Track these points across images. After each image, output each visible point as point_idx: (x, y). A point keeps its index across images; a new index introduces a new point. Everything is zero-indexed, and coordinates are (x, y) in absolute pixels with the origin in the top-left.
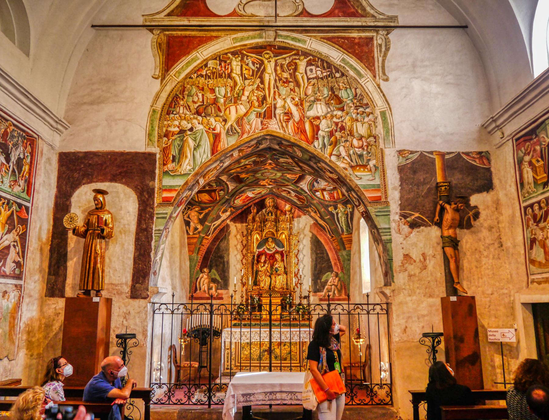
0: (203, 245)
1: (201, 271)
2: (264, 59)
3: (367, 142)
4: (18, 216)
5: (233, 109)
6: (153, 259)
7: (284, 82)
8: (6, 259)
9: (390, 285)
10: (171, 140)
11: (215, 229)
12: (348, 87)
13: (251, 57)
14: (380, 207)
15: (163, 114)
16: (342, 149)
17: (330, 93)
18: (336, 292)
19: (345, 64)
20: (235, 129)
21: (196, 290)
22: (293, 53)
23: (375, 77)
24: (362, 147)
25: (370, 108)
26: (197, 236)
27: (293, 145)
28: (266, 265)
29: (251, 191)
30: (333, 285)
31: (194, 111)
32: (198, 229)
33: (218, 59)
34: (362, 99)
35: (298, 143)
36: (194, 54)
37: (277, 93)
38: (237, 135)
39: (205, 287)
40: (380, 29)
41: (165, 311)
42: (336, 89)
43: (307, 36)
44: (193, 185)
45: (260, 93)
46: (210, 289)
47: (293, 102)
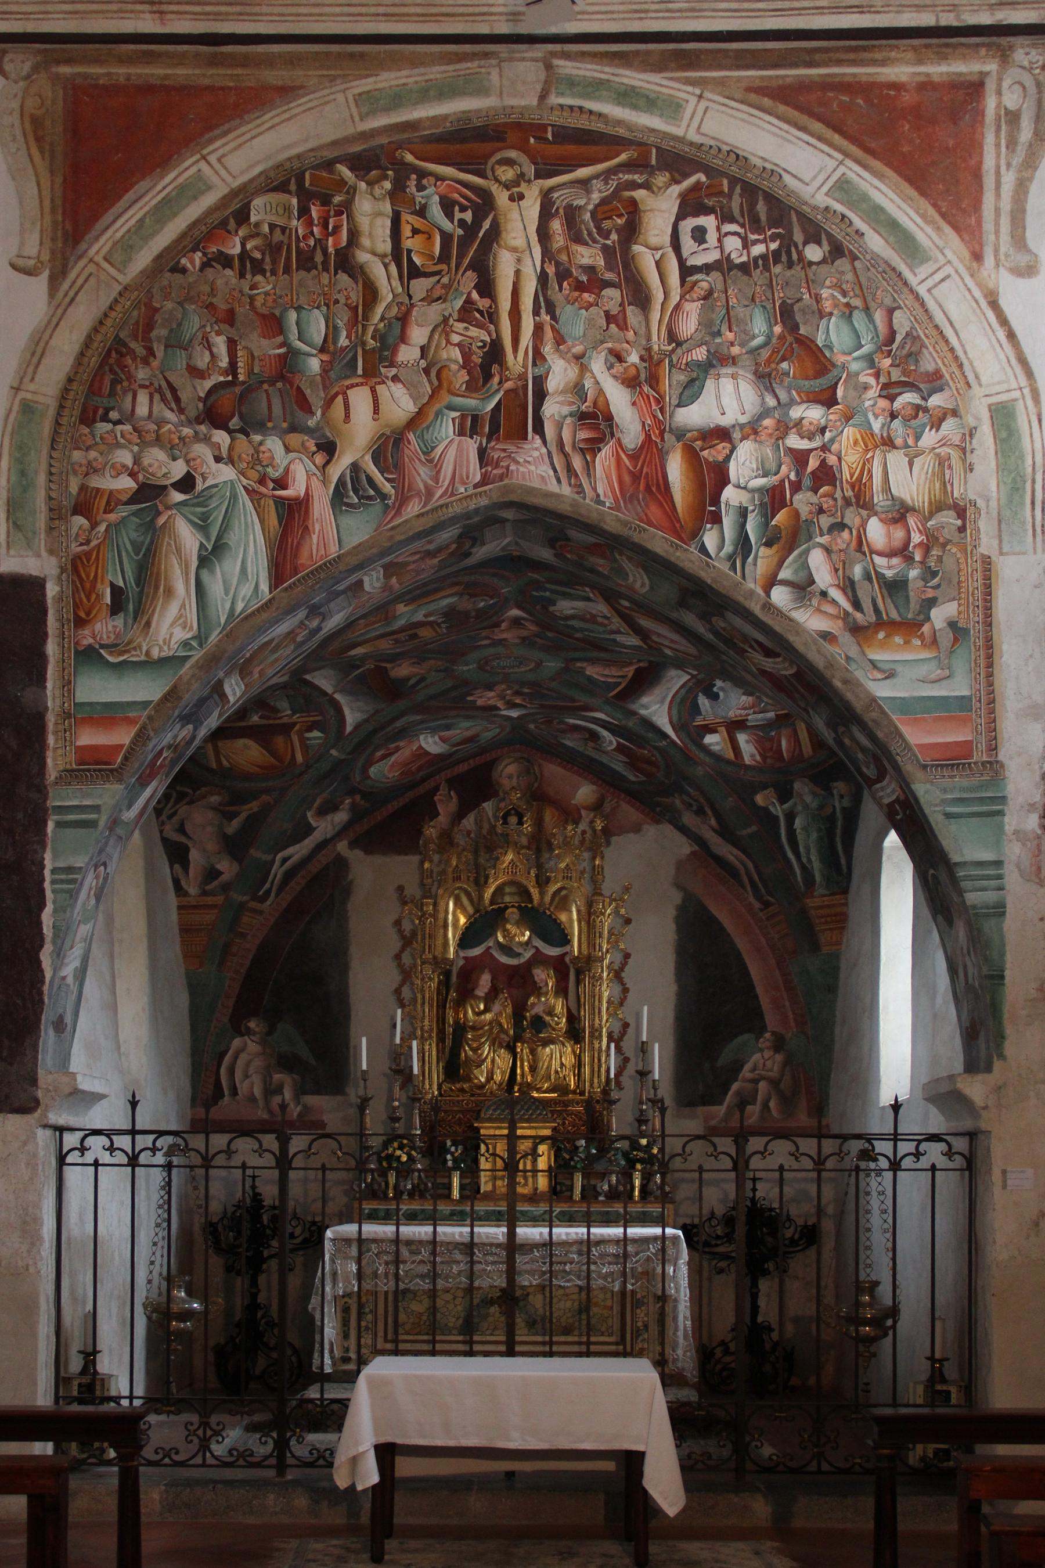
0: (243, 936)
1: (238, 1028)
2: (495, 188)
3: (925, 531)
5: (360, 399)
6: (48, 975)
7: (580, 287)
9: (989, 1069)
10: (102, 528)
11: (289, 876)
12: (857, 302)
13: (440, 178)
14: (965, 783)
15: (64, 421)
16: (818, 561)
17: (778, 329)
18: (772, 1104)
19: (851, 205)
20: (370, 481)
21: (218, 1093)
22: (623, 157)
23: (977, 257)
24: (903, 552)
25: (946, 393)
26: (219, 899)
27: (612, 544)
28: (497, 1007)
29: (434, 731)
30: (762, 1078)
31: (195, 408)
32: (220, 873)
33: (293, 187)
34: (914, 356)
35: (636, 538)
36: (188, 168)
37: (548, 334)
38: (377, 507)
39: (252, 1085)
40: (1019, 40)
41: (106, 1158)
42: (803, 311)
43: (688, 82)
44: (202, 701)
45: (474, 332)
46: (271, 1090)
47: (618, 368)
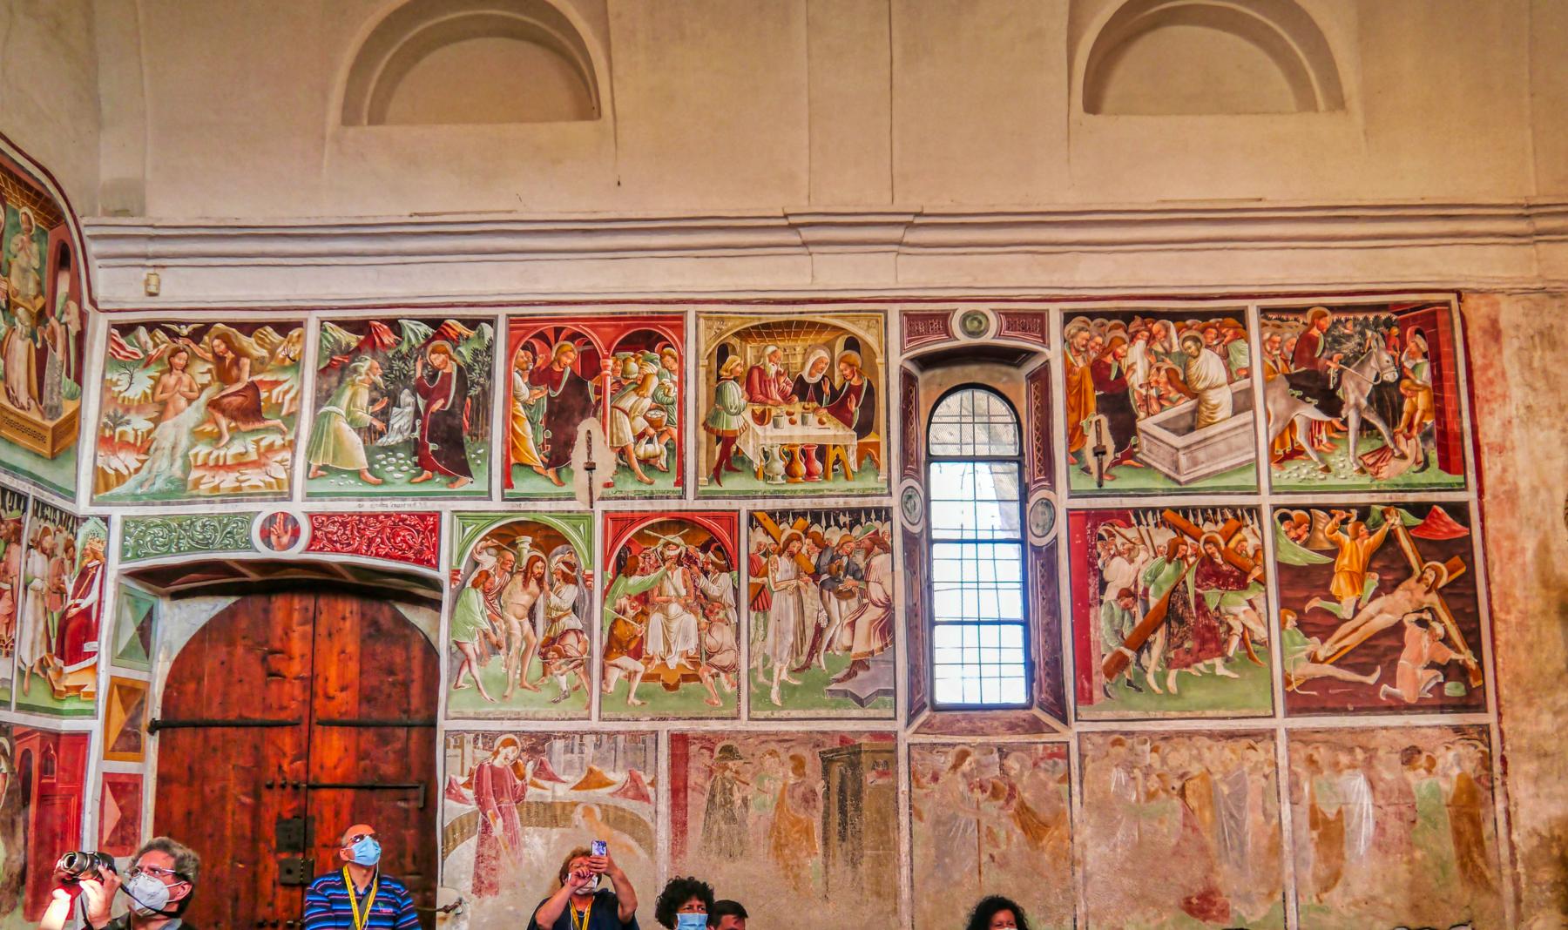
4: (1414, 541)
8: (1394, 663)
